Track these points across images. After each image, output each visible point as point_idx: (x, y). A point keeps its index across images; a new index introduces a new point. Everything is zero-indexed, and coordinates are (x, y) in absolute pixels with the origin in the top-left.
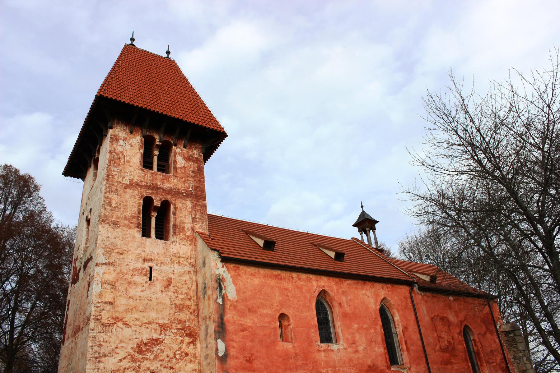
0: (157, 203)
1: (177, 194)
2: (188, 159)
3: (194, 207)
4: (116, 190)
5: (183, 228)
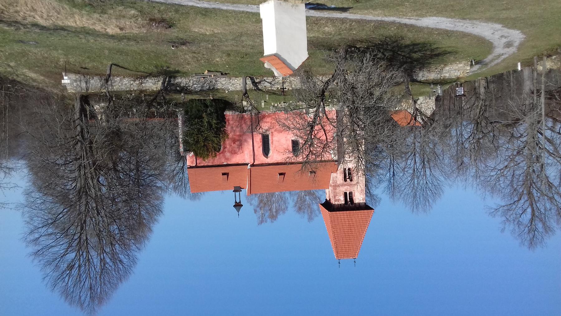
0: (348, 180)
1: (343, 185)
2: (339, 200)
3: (336, 182)
5: (340, 173)
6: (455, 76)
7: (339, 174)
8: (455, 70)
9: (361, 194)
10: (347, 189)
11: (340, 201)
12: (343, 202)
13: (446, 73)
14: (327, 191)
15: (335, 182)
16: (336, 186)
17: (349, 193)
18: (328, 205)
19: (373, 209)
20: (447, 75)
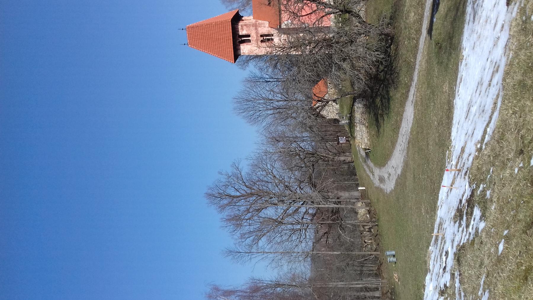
1: (257, 33)
2: (242, 29)
3: (260, 27)
4: (261, 51)
5: (268, 30)
6: (357, 135)
7: (267, 29)
8: (362, 136)
9: (249, 51)
10: (253, 37)
11: (241, 30)
12: (240, 34)
13: (360, 128)
14: (251, 17)
15: (260, 25)
16: (256, 26)
17: (249, 39)
18: (237, 18)
19: (235, 62)
20: (358, 129)
